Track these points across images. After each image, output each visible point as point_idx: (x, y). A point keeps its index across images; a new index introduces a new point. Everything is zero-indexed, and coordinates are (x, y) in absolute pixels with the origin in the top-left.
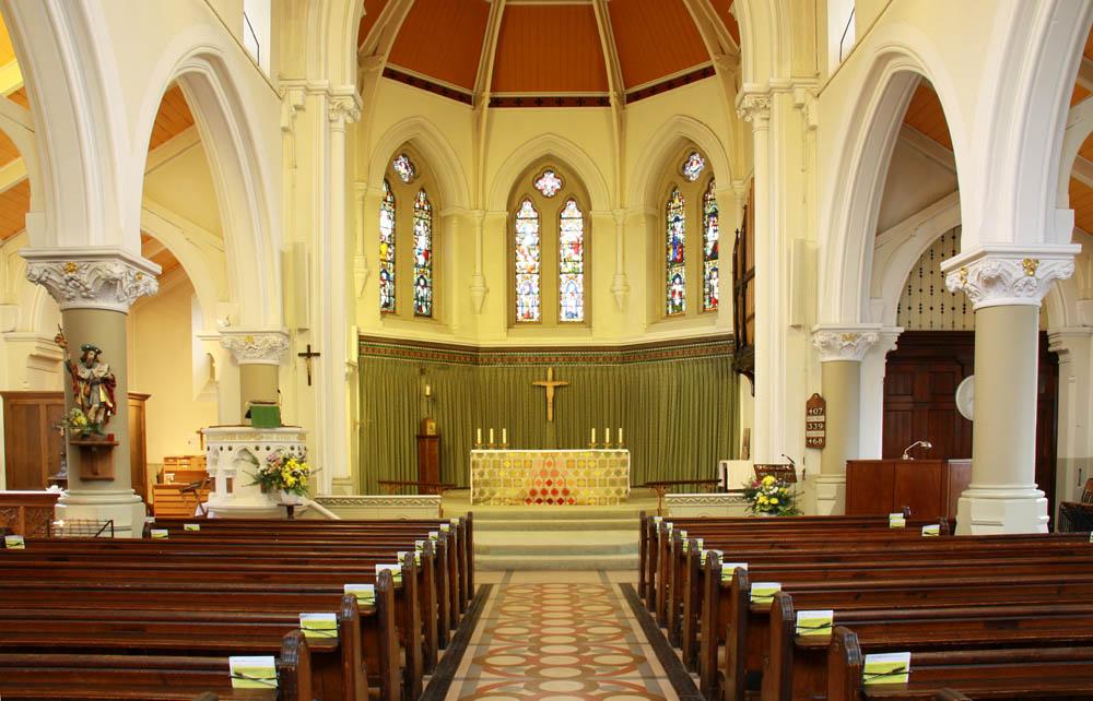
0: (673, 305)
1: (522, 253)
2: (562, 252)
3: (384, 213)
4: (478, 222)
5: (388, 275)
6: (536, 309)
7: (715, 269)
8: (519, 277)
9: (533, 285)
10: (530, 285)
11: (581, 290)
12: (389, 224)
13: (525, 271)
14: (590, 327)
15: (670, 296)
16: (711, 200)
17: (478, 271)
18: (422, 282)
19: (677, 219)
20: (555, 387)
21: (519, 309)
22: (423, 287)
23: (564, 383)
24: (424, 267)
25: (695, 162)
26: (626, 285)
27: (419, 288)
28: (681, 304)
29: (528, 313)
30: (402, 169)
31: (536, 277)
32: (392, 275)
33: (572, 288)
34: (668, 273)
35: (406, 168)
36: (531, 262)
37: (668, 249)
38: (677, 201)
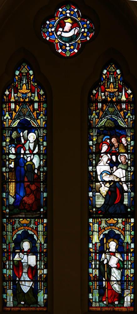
0: (17, 292)
16: (104, 102)
19: (25, 126)
25: (68, 26)
28: (34, 291)
37: (6, 182)
38: (24, 89)
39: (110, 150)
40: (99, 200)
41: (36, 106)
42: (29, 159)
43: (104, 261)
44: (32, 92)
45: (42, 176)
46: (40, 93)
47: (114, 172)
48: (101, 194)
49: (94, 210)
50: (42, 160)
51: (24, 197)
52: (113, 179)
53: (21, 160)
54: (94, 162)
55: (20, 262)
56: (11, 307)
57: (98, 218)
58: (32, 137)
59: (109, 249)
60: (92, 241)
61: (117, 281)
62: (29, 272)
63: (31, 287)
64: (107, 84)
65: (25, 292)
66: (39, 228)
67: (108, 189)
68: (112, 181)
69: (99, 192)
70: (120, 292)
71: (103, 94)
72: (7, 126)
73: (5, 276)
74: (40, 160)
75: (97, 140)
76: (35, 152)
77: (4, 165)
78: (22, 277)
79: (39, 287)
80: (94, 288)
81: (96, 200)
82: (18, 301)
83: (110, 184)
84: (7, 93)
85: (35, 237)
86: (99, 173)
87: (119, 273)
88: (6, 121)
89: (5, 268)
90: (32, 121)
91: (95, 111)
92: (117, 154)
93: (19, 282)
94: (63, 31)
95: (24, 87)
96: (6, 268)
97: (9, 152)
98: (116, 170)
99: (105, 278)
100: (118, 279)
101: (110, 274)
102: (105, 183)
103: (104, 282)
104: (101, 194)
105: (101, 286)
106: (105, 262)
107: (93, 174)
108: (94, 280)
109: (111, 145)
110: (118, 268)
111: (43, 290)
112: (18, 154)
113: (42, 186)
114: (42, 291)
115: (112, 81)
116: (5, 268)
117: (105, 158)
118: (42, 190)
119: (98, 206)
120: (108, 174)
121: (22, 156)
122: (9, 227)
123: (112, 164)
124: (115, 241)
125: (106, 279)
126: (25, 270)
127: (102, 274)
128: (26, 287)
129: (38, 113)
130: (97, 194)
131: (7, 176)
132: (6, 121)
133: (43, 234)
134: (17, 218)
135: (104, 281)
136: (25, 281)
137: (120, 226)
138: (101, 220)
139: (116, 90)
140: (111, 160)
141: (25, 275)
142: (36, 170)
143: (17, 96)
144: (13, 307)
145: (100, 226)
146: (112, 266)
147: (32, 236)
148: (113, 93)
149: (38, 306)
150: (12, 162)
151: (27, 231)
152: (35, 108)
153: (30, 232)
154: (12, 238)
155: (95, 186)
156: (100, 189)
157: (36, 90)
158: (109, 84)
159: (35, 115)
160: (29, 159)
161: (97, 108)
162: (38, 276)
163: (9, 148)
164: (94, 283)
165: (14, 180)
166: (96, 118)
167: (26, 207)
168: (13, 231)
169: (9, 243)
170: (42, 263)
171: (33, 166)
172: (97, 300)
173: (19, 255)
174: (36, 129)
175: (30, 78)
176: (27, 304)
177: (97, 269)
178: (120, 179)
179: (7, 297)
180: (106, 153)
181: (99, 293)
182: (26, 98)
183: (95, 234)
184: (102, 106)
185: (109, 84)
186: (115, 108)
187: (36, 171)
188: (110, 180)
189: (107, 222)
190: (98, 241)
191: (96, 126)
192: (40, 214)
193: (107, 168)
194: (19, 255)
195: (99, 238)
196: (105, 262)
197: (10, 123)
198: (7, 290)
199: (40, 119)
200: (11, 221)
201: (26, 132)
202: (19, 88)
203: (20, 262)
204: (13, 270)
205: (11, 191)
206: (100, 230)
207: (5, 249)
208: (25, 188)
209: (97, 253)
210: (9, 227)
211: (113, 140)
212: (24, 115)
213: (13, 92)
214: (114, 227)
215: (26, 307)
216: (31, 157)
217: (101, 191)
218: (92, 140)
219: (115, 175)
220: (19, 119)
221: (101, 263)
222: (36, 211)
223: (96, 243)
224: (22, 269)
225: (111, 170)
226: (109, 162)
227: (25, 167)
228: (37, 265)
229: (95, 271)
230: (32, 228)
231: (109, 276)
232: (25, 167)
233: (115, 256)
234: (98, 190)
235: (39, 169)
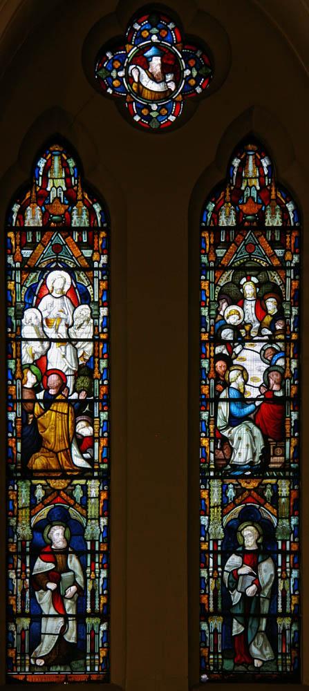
5: (75, 531)
18: (249, 537)
22: (252, 559)
24: (259, 469)
27: (234, 560)
32: (95, 529)
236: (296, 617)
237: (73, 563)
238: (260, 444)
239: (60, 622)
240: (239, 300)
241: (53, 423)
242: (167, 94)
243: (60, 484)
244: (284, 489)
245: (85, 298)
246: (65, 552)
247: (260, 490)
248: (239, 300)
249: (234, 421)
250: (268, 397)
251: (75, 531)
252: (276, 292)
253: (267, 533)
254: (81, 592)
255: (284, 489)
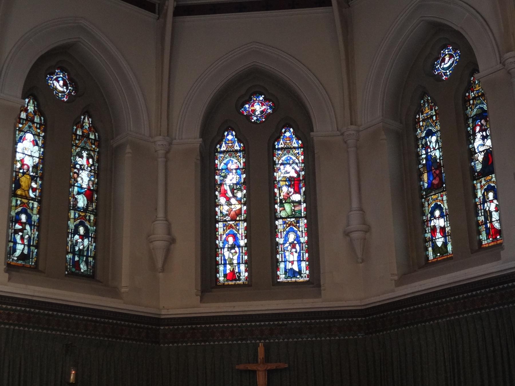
0: (435, 246)
1: (224, 194)
2: (276, 190)
3: (29, 137)
4: (161, 152)
5: (29, 217)
6: (243, 267)
7: (489, 189)
8: (220, 225)
9: (239, 236)
10: (235, 236)
11: (304, 239)
12: (36, 152)
13: (228, 218)
14: (319, 286)
15: (428, 235)
16: (474, 98)
17: (161, 214)
18: (82, 230)
19: (430, 133)
20: (270, 373)
21: (221, 268)
22: (82, 237)
23: (283, 365)
24: (85, 210)
25: (447, 59)
26: (364, 222)
27: (77, 237)
28: (445, 244)
29: (233, 272)
30: (59, 85)
31: (243, 225)
32: (35, 218)
33: (292, 237)
34: (423, 206)
35: (65, 84)
36: (236, 206)
37: (421, 174)
38: (427, 110)
39: (481, 129)
40: (479, 166)
41: (434, 118)
42: (433, 155)
43: (486, 208)
44: (431, 110)
45: (442, 162)
46: (436, 109)
47: (485, 143)
48: (479, 161)
49: (476, 174)
50: (441, 152)
51: (433, 180)
52: (485, 149)
53: (429, 157)
54: (472, 141)
55: (434, 226)
56: (432, 260)
57: (479, 179)
58: (434, 139)
59: (488, 199)
60: (477, 196)
61: (497, 220)
62: (441, 231)
63: (443, 242)
64: (474, 86)
65: (440, 246)
66: (443, 199)
67: (483, 156)
68: (485, 150)
69: (478, 160)
70: (500, 229)
71: (473, 93)
72: (419, 137)
73: (427, 238)
74: (440, 152)
75: (472, 126)
76: (436, 148)
77: (420, 164)
78: (437, 236)
79: (447, 240)
80: (482, 231)
81: (477, 167)
82: (436, 255)
83: (484, 152)
84: (418, 116)
85: (442, 206)
86: (476, 148)
87: (497, 214)
88: (418, 135)
89: (426, 233)
90: (433, 129)
91: (469, 107)
92: (485, 130)
93: (435, 240)
94: (444, 64)
95: (427, 108)
96: (426, 233)
97: (422, 154)
98: (486, 141)
99: (489, 221)
100: (497, 219)
101: (491, 217)
102: (480, 153)
103: (488, 224)
104: (479, 161)
105: (486, 227)
106: (487, 209)
107: (473, 149)
108: (482, 225)
109: (482, 125)
110: (496, 211)
111: (450, 241)
112: (427, 153)
113: (443, 169)
114: (450, 242)
115: (477, 83)
116: (426, 233)
117: (479, 136)
118: (443, 172)
119: (478, 171)
120: (482, 146)
121: (429, 154)
122: (426, 204)
123: (484, 138)
124: (492, 191)
125: (489, 221)
126: (438, 231)
127: (486, 219)
128: (439, 242)
129: (436, 122)
130: (476, 162)
131: (422, 170)
132: (418, 135)
133: (446, 202)
134: (430, 196)
135: (488, 223)
136: (438, 238)
137: (494, 180)
138: (429, 198)
139: (480, 87)
140: (483, 136)
141: (439, 234)
142: (438, 160)
143: (423, 116)
144: (433, 259)
145: (481, 184)
146: (492, 211)
147: (440, 205)
148: (479, 90)
149: (448, 254)
150: (424, 160)
151: (437, 203)
152: (434, 120)
153: (439, 203)
154: (429, 210)
155: (475, 157)
156: (478, 158)
157: (433, 108)
158: (475, 85)
159: (434, 124)
160: (433, 155)
161: (470, 104)
162: (447, 232)
163: (421, 151)
164: (482, 226)
165: (426, 171)
166: (470, 111)
167: (435, 187)
168: (428, 206)
169: (427, 215)
170: (448, 222)
171: (436, 158)
172: (486, 239)
173: (433, 221)
174: (435, 132)
175: (429, 102)
176: (442, 255)
177: (482, 216)
178: (490, 146)
179: (429, 253)
180: (479, 132)
181: (486, 233)
182: (428, 116)
183: (479, 191)
184: (473, 102)
185: (475, 85)
186: (481, 99)
187: (438, 161)
188: (484, 149)
189: (485, 180)
190: (481, 195)
191: (471, 116)
192: (444, 188)
193: (481, 142)
194: (433, 221)
195: (481, 193)
196: (487, 209)
197: (420, 135)
198: (428, 248)
199: (437, 125)
200: (427, 199)
201: (430, 137)
202: (424, 110)
203: (434, 226)
204: (431, 233)
205: (425, 179)
206: (481, 187)
207: (425, 220)
208: (433, 174)
209: (482, 204)
210: (426, 204)
211: (483, 121)
212: (428, 126)
213: (420, 114)
214: (490, 182)
215: (441, 257)
216: (434, 152)
217: (479, 160)
218: (470, 127)
219: (486, 145)
220: (426, 130)
221: (485, 211)
222: (441, 188)
223: (480, 197)
224: (436, 230)
225: (484, 143)
226: (481, 137)
227: (432, 160)
228: (445, 225)
229: (482, 217)
230: (440, 200)
231: (491, 218)
232: (432, 160)
233: (493, 202)
234: (476, 159)
235: (439, 159)
236: (94, 258)
237: (28, 227)
238: (86, 202)
239: (22, 246)
240: (81, 157)
241: (24, 181)
242: (63, 92)
243: (25, 201)
244: (92, 218)
245: (37, 144)
246: (25, 224)
247: (85, 216)
248: (81, 157)
249: (79, 193)
250: (89, 189)
251: (29, 217)
252: (92, 158)
253: (87, 230)
254: (30, 238)
255: (92, 218)
